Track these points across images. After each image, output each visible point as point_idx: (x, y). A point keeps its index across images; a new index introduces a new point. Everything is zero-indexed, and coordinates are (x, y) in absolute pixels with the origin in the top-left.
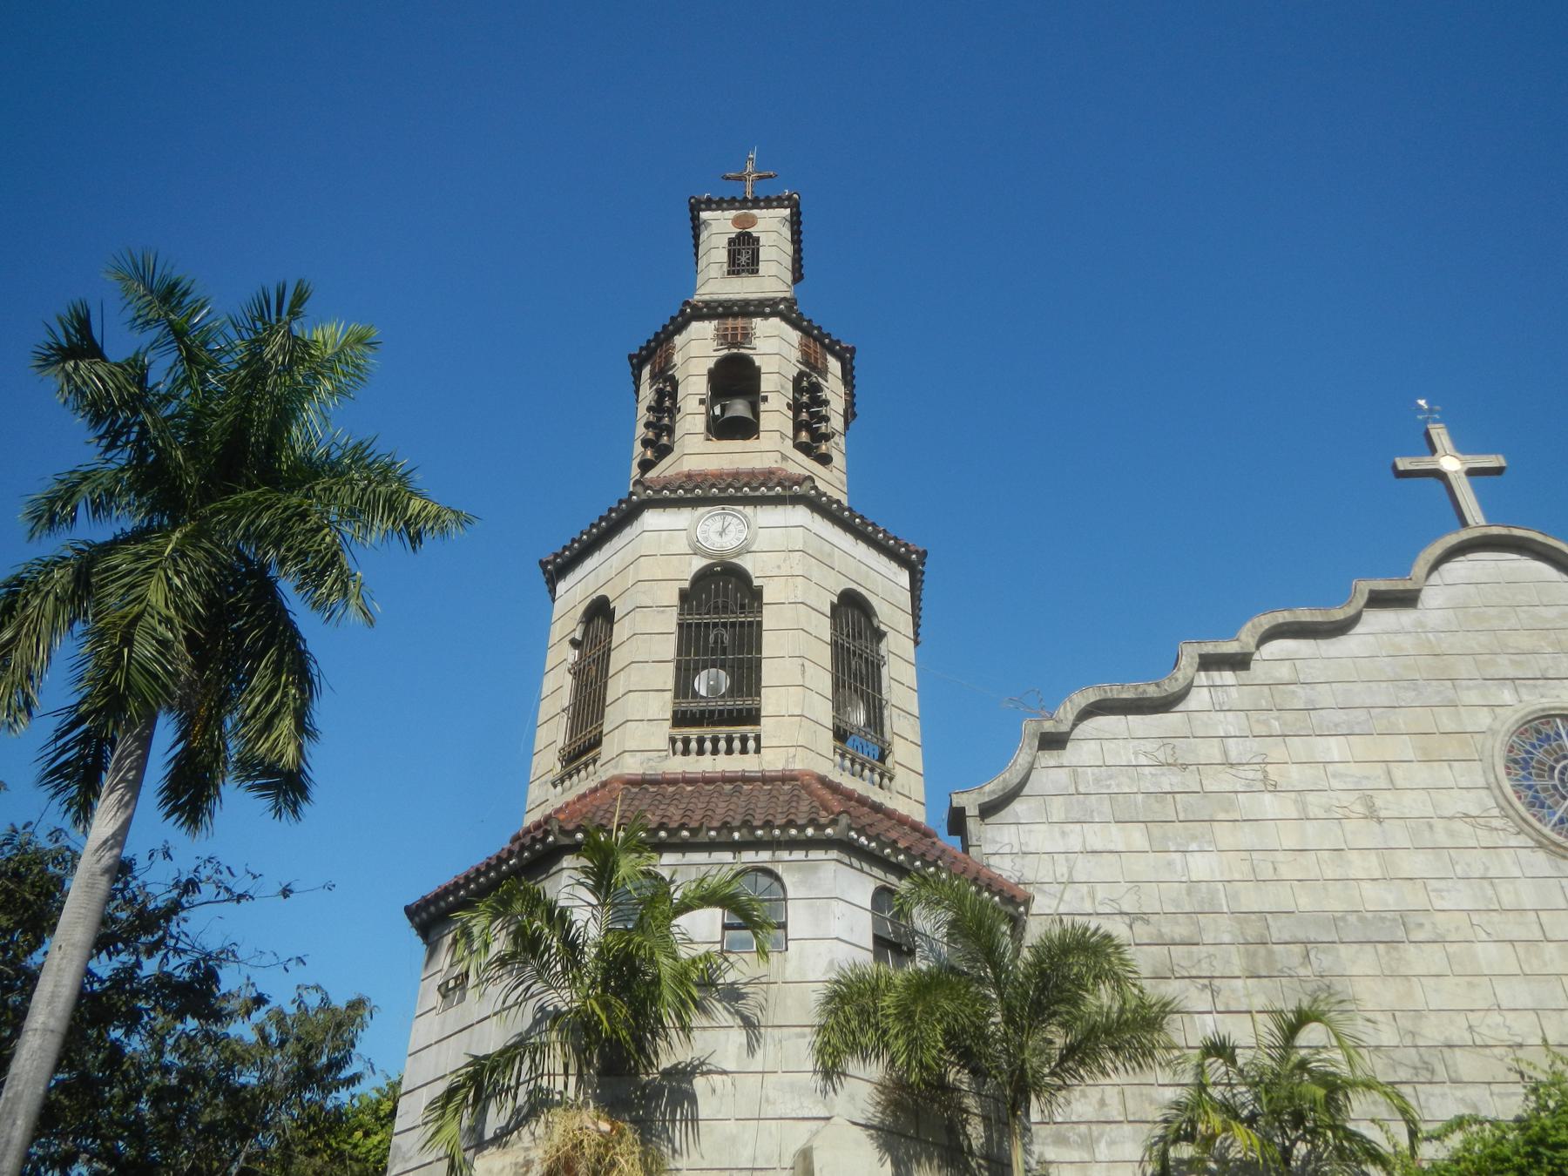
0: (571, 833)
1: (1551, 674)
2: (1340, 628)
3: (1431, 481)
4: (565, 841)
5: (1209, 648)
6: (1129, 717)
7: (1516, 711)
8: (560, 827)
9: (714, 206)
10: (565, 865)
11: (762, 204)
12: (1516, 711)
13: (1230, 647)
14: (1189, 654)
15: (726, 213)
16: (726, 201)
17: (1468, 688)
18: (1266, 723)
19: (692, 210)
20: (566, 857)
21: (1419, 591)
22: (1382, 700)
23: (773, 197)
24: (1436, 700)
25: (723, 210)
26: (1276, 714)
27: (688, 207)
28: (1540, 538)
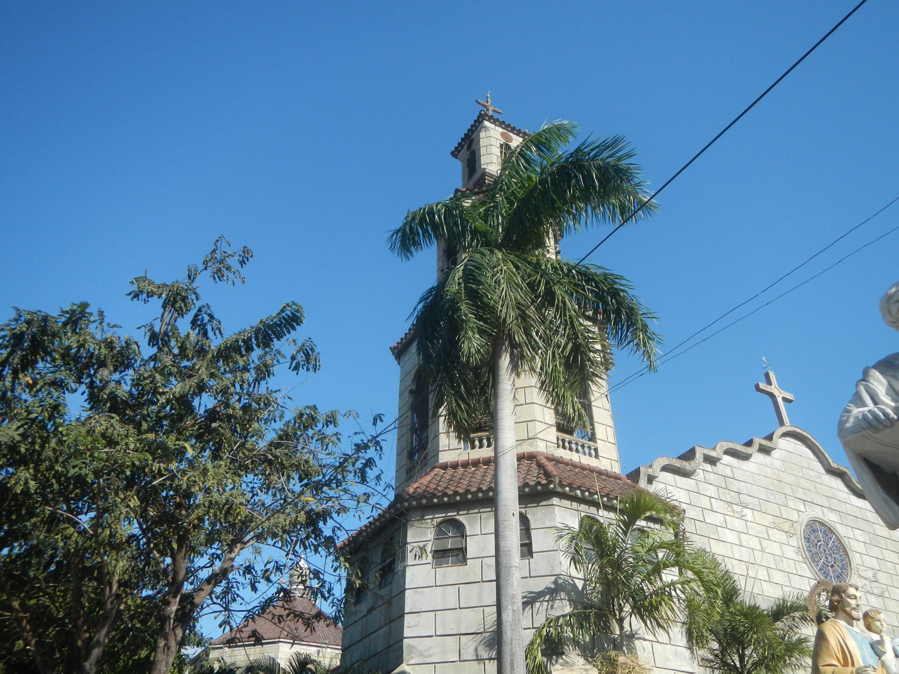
0: (563, 486)
1: (815, 502)
2: (746, 457)
3: (767, 397)
4: (559, 489)
5: (706, 452)
6: (676, 476)
7: (806, 516)
8: (560, 481)
9: (492, 121)
10: (555, 503)
11: (515, 132)
12: (806, 516)
13: (713, 454)
14: (699, 453)
15: (497, 127)
16: (499, 122)
17: (790, 500)
18: (724, 494)
19: (479, 117)
20: (554, 498)
21: (775, 449)
22: (763, 496)
23: (523, 131)
24: (780, 502)
25: (496, 125)
26: (728, 491)
27: (478, 114)
28: (812, 439)
